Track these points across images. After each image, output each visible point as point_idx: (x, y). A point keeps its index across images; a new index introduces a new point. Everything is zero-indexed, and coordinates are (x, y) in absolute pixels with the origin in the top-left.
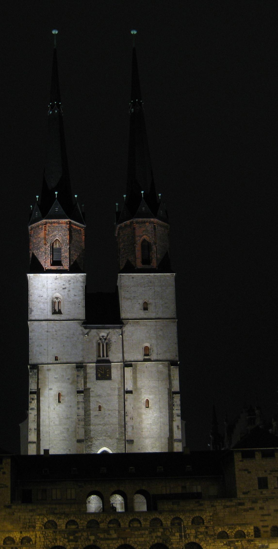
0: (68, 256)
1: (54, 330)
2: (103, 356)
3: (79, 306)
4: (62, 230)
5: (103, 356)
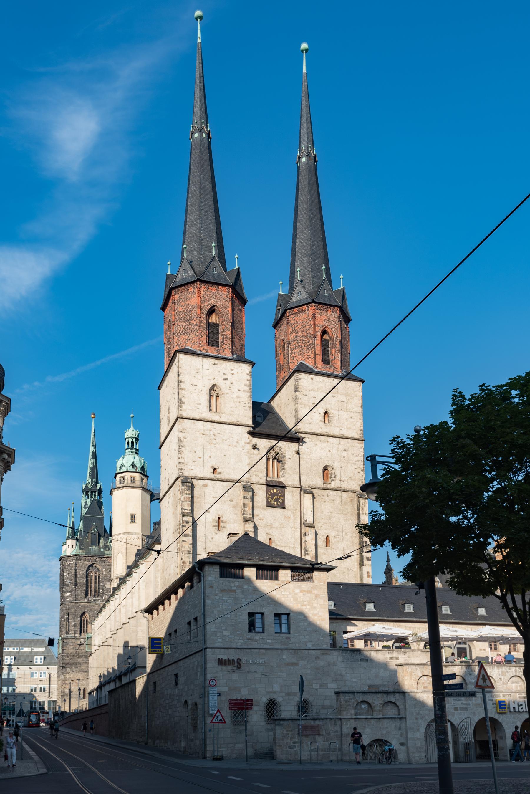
1: (212, 433)
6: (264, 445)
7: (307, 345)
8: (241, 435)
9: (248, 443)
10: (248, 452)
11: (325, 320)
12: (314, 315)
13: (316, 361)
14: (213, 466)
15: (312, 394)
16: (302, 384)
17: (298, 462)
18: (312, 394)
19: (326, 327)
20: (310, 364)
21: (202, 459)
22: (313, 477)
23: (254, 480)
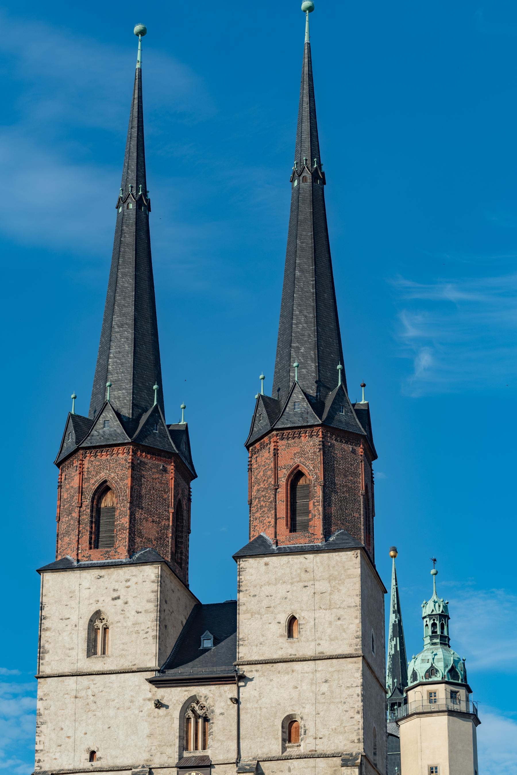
0: (127, 525)
1: (90, 693)
2: (196, 748)
3: (147, 635)
4: (116, 468)
5: (196, 748)
6: (177, 698)
7: (268, 504)
8: (138, 688)
9: (149, 700)
10: (149, 715)
11: (295, 454)
12: (276, 450)
13: (278, 531)
14: (89, 749)
15: (267, 590)
16: (248, 577)
17: (236, 718)
18: (267, 590)
19: (298, 466)
20: (269, 536)
21: (72, 739)
22: (263, 740)
23: (156, 762)
